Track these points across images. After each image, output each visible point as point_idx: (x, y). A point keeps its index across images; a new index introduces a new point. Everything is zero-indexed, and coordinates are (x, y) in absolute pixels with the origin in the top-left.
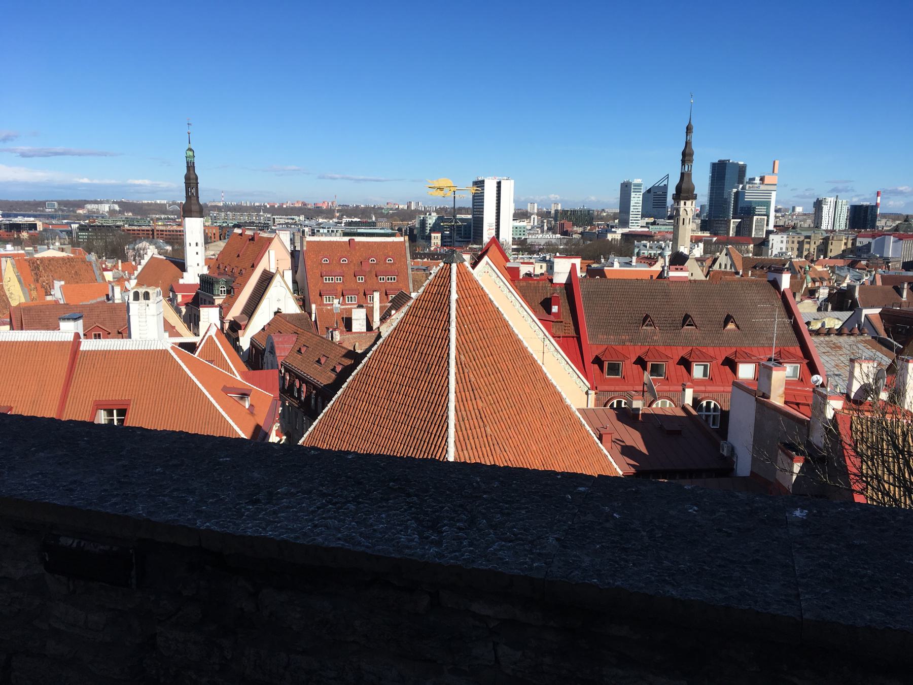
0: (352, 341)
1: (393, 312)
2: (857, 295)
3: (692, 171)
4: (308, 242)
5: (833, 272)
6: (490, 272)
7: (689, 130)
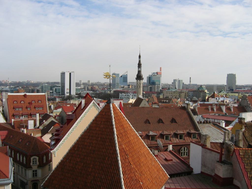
0: (30, 133)
1: (44, 121)
2: (197, 110)
4: (9, 96)
5: (250, 104)
6: (95, 106)
7: (140, 57)
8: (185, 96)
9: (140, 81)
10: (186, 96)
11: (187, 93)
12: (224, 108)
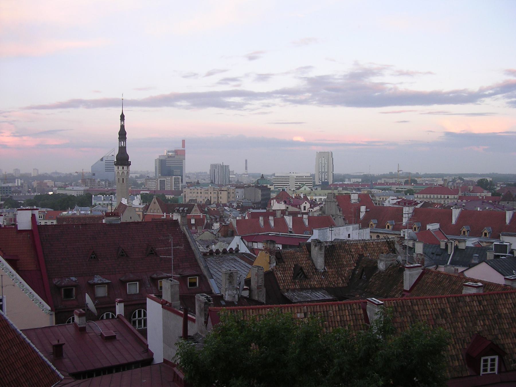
3: (126, 146)
7: (122, 117)
8: (229, 197)
9: (123, 168)
10: (231, 198)
11: (232, 191)
12: (289, 220)
